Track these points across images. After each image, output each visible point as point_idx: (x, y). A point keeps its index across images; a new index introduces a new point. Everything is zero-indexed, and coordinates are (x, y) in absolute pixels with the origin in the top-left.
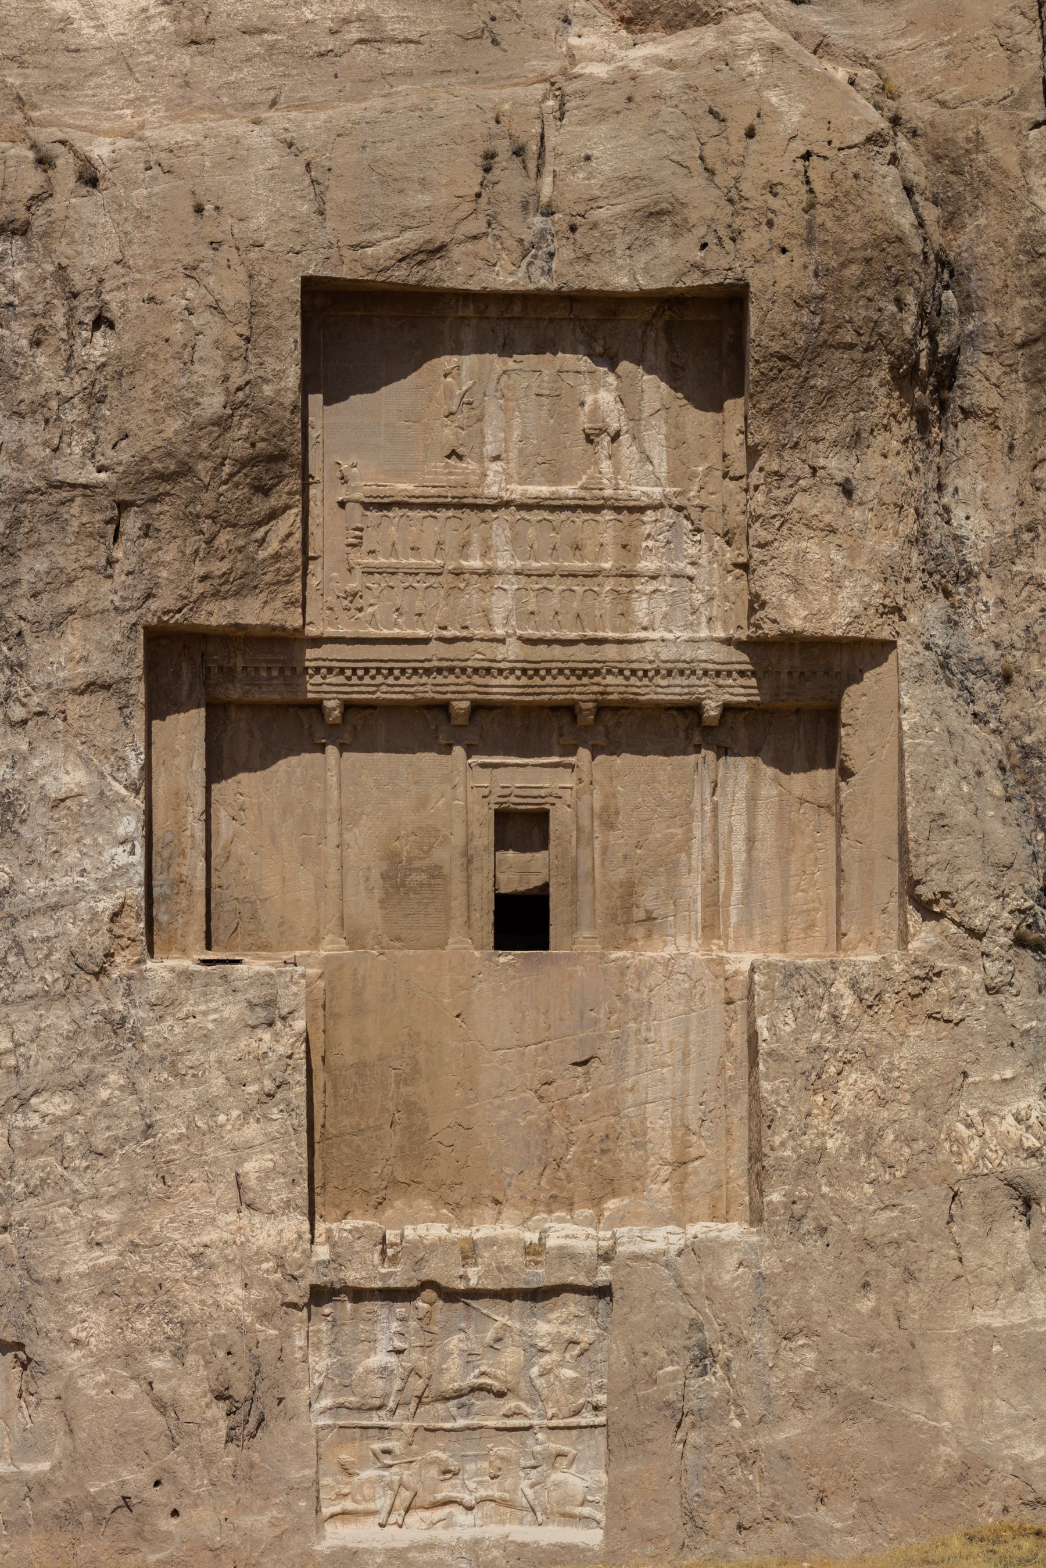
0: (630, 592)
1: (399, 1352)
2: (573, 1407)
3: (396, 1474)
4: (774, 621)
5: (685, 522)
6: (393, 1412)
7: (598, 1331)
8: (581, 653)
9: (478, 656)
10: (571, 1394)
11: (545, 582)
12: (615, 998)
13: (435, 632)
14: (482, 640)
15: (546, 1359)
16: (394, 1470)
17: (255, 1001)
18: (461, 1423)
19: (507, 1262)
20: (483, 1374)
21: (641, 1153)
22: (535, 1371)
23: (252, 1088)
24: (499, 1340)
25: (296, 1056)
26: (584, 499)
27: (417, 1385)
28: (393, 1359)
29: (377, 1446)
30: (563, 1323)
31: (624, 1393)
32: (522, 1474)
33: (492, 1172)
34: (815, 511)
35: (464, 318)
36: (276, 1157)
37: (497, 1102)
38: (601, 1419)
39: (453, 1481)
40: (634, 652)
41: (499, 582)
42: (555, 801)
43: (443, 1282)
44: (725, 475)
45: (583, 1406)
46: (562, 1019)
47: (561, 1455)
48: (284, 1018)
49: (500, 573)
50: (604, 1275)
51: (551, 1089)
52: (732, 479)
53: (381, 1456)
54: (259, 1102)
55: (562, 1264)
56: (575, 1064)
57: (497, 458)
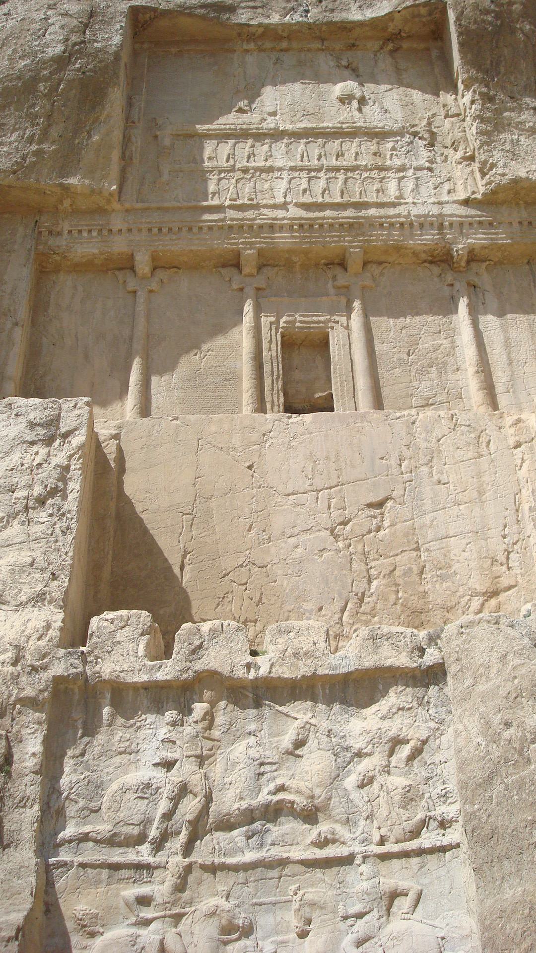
0: (384, 178)
1: (168, 765)
2: (409, 826)
3: (155, 933)
4: (503, 175)
5: (420, 141)
6: (158, 845)
7: (432, 724)
8: (350, 213)
9: (261, 217)
10: (404, 807)
11: (313, 174)
12: (405, 448)
13: (227, 203)
14: (266, 206)
15: (364, 766)
16: (153, 926)
17: (37, 421)
18: (249, 856)
19: (306, 646)
20: (282, 788)
21: (449, 584)
22: (350, 782)
23: (21, 494)
24: (300, 744)
25: (72, 467)
26: (341, 128)
27: (190, 807)
28: (159, 774)
29: (131, 892)
30: (383, 718)
31: (488, 781)
32: (343, 926)
33: (289, 608)
34: (519, 120)
35: (247, 51)
36: (38, 554)
37: (293, 540)
38: (454, 835)
39: (243, 942)
40: (392, 211)
41: (277, 174)
42: (333, 324)
43: (225, 670)
44: (447, 116)
45: (424, 823)
46: (353, 466)
47: (394, 895)
48: (65, 436)
49: (280, 169)
50: (431, 657)
51: (348, 527)
52: (452, 116)
53: (135, 906)
54: (27, 508)
55: (377, 647)
56: (370, 506)
57: (274, 114)
